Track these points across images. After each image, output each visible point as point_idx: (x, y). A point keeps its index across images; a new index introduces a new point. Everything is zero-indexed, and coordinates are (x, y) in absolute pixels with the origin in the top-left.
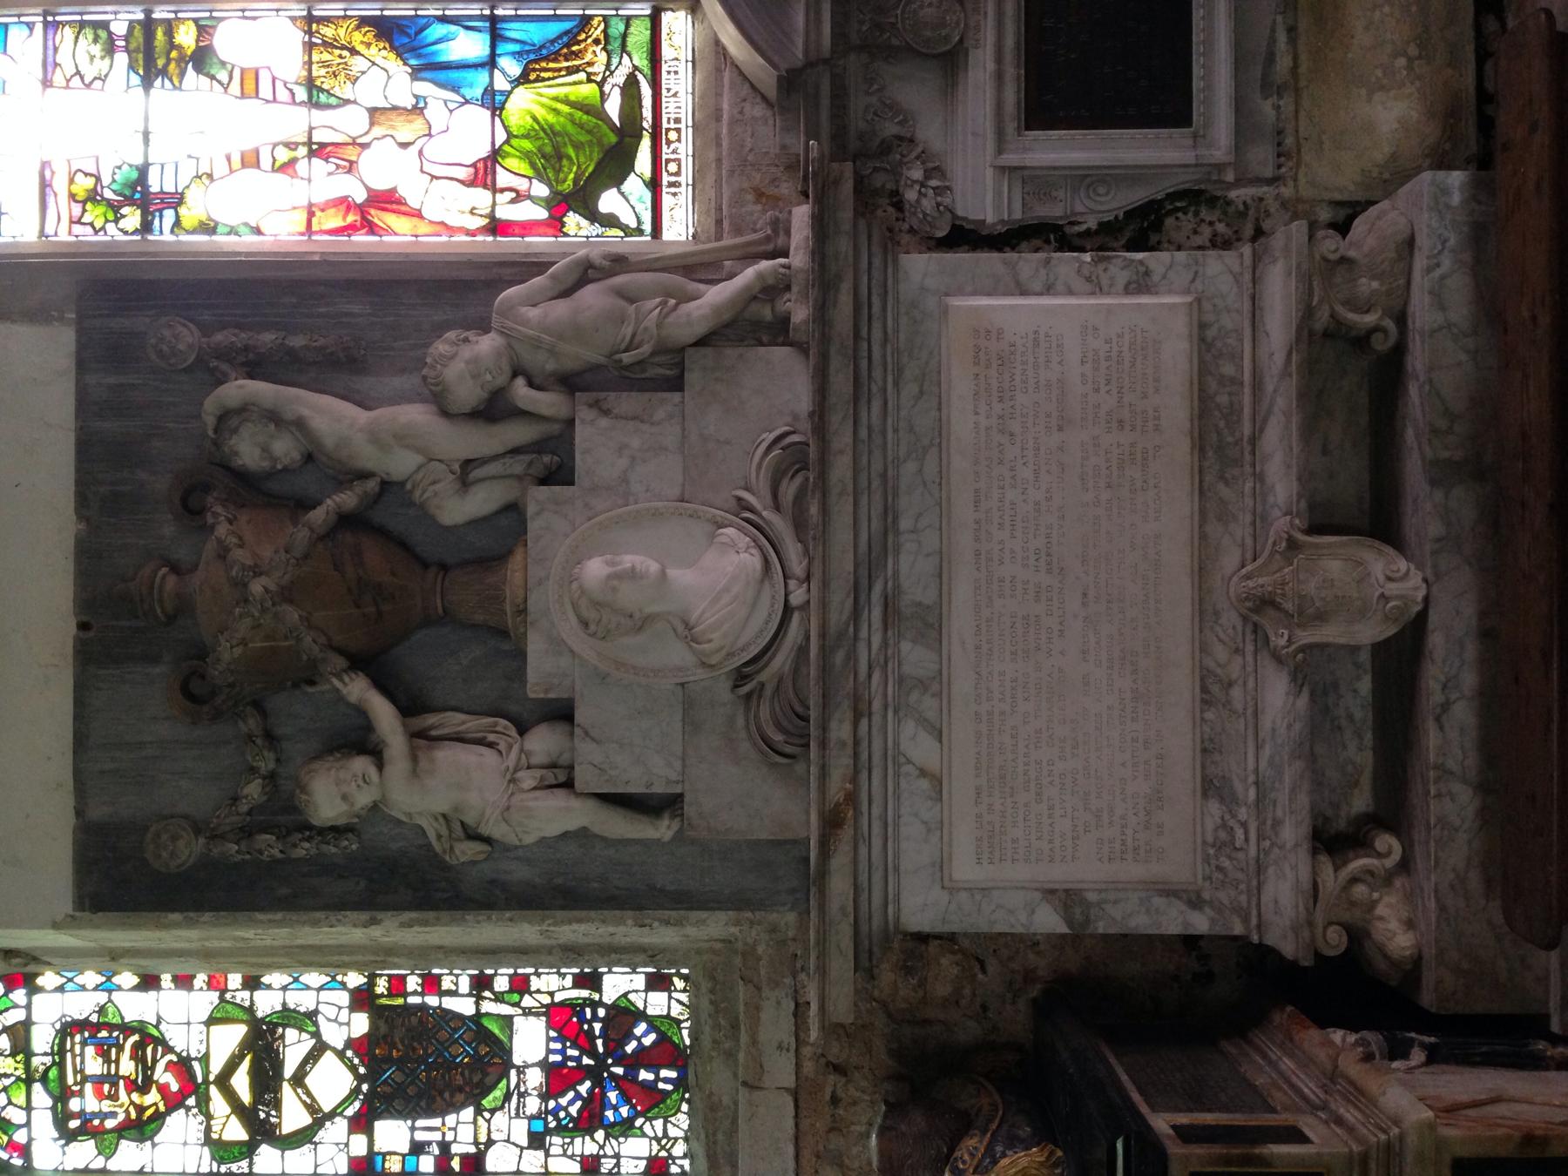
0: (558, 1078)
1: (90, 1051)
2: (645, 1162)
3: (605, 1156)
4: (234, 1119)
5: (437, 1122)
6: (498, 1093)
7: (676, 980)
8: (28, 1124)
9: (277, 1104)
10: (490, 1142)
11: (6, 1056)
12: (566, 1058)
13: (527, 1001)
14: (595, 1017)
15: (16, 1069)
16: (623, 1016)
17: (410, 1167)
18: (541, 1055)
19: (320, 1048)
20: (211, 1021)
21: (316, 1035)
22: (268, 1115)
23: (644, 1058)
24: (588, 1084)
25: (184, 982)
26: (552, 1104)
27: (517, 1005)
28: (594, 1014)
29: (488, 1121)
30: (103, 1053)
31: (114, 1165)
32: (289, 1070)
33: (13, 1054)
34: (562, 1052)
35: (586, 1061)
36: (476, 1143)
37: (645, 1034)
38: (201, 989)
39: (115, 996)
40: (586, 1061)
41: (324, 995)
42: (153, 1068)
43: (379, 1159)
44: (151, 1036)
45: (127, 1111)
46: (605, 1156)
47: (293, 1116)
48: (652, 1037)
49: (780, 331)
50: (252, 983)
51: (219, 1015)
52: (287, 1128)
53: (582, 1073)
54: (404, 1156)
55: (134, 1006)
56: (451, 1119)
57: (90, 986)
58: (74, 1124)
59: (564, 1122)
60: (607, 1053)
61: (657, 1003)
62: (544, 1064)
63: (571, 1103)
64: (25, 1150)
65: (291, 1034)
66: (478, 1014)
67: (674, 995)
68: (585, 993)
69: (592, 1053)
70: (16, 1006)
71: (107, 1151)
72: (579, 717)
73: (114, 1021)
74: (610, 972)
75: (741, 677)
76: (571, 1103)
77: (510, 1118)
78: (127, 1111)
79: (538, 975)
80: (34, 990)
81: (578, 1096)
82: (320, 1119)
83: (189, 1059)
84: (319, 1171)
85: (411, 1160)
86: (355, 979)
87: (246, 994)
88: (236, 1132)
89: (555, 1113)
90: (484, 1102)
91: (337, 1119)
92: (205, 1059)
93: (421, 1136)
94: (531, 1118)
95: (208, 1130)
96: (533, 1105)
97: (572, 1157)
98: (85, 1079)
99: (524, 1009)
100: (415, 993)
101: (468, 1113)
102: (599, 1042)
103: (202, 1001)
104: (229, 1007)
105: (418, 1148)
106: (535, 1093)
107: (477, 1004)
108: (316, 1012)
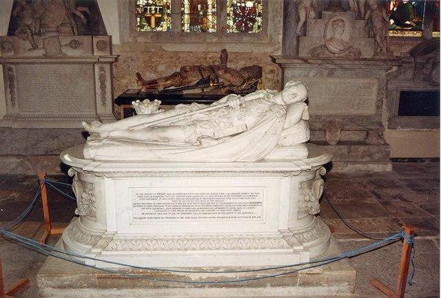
0: (243, 9)
16: (254, 21)
23: (246, 25)
49: (376, 54)
53: (244, 13)
69: (247, 15)
72: (319, 20)
75: (325, 46)
96: (239, 4)
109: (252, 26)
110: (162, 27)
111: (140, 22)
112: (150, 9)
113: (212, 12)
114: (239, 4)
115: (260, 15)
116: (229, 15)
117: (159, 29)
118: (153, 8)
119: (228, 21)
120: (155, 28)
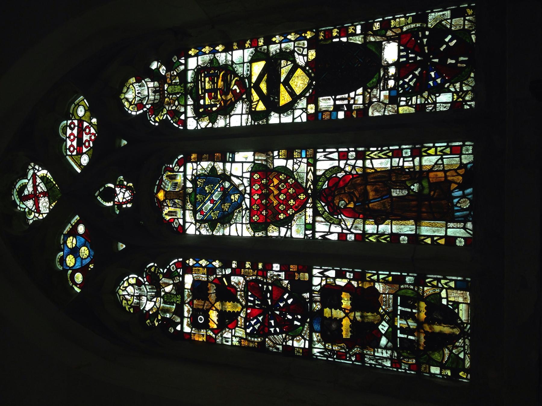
1: (207, 79)
2: (449, 105)
3: (429, 103)
4: (260, 102)
5: (346, 96)
6: (374, 80)
7: (468, 10)
8: (185, 113)
9: (278, 94)
10: (371, 103)
11: (178, 85)
12: (408, 58)
13: (389, 33)
14: (424, 36)
15: (181, 90)
17: (333, 118)
18: (396, 58)
19: (296, 66)
20: (251, 62)
21: (294, 61)
22: (274, 99)
23: (451, 52)
24: (419, 70)
25: (242, 47)
26: (401, 82)
27: (384, 35)
28: (424, 34)
29: (370, 93)
30: (212, 80)
31: (216, 126)
32: (283, 77)
33: (180, 85)
34: (406, 56)
35: (419, 58)
36: (364, 103)
37: (451, 40)
38: (248, 48)
39: (217, 55)
40: (419, 58)
41: (297, 43)
42: (230, 84)
43: (320, 114)
44: (230, 70)
45: (221, 104)
46: (429, 103)
47: (285, 98)
48: (455, 41)
50: (268, 42)
51: (255, 58)
52: (282, 103)
53: (417, 65)
54: (331, 112)
55: (222, 58)
56: (352, 94)
57: (207, 52)
58: (201, 110)
59: (407, 90)
60: (429, 53)
61: (458, 22)
62: (396, 64)
63: (411, 80)
64: (184, 123)
65: (283, 62)
66: (366, 43)
67: (467, 18)
68: (418, 25)
70: (182, 64)
71: (213, 120)
73: (216, 66)
74: (432, 12)
76: (411, 80)
77: (380, 91)
78: (221, 104)
79: (394, 19)
80: (188, 56)
81: (415, 76)
82: (295, 98)
83: (244, 78)
84: (296, 121)
85: (335, 113)
86: (309, 35)
87: (265, 47)
88: (261, 107)
89: (402, 86)
90: (368, 85)
91: (302, 98)
92: (250, 77)
93: (338, 102)
94: (390, 90)
95: (251, 107)
97: (411, 106)
98: (206, 91)
99: (387, 37)
100: (336, 37)
101: (360, 91)
102: (426, 48)
103: (248, 53)
104: (259, 54)
105: (337, 108)
106: (393, 78)
107: (365, 38)
108: (294, 51)
109: (455, 35)
110: (456, 304)
111: (443, 367)
112: (403, 331)
113: (413, 156)
114: (391, 83)
115: (422, 18)
116: (420, 108)
117: (463, 313)
118: (400, 323)
119: (441, 108)
120: (461, 325)
